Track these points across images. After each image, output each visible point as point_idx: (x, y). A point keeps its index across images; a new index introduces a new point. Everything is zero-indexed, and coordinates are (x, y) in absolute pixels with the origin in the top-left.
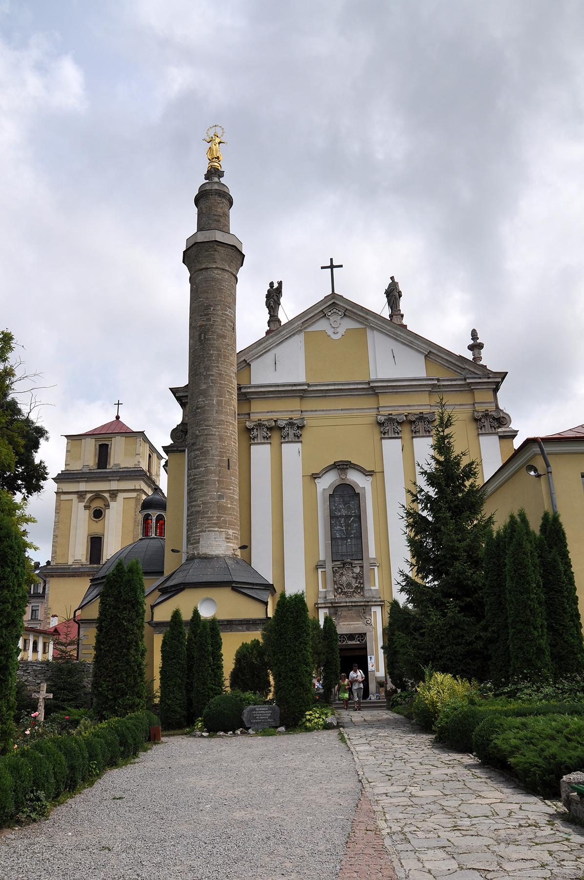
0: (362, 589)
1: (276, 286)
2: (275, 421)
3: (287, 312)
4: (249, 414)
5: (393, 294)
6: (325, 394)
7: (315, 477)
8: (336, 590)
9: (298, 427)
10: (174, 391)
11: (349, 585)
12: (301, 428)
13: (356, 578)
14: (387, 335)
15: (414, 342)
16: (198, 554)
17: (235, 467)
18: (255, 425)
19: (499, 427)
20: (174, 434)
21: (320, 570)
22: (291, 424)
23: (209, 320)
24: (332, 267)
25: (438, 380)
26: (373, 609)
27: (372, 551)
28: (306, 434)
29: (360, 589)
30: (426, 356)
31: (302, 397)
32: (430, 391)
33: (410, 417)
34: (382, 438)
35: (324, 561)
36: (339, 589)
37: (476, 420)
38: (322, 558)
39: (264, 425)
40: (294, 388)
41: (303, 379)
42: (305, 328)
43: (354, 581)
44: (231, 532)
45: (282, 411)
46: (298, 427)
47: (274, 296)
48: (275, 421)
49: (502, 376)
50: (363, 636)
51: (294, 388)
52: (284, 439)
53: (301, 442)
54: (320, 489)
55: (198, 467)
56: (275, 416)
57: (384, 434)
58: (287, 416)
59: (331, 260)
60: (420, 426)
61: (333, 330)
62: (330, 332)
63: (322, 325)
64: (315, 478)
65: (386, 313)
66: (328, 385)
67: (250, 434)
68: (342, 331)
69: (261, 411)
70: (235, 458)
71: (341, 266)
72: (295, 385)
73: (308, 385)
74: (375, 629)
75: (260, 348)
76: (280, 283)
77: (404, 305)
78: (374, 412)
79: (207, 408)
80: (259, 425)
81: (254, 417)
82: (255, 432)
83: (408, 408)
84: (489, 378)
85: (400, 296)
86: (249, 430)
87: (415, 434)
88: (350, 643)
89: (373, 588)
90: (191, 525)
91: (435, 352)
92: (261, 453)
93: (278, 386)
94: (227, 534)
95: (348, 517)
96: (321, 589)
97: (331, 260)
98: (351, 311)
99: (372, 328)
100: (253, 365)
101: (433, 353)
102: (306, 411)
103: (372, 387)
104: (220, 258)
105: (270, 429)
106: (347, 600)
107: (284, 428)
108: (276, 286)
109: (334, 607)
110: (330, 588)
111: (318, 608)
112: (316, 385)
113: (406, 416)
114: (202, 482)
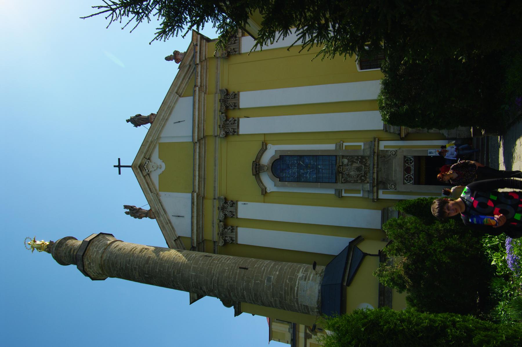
0: (363, 157)
1: (128, 210)
2: (220, 221)
3: (143, 204)
4: (214, 242)
5: (137, 121)
6: (202, 179)
7: (264, 192)
8: (363, 181)
9: (226, 202)
10: (193, 301)
11: (358, 169)
12: (226, 200)
13: (353, 162)
14: (163, 127)
15: (168, 105)
16: (318, 308)
17: (248, 262)
18: (222, 238)
19: (236, 37)
20: (227, 304)
21: (344, 194)
22: (223, 209)
23: (135, 268)
24: (119, 166)
25: (195, 86)
26: (382, 148)
27: (331, 147)
28: (231, 197)
29: (362, 159)
30: (180, 96)
31: (204, 198)
32: (205, 93)
33: (223, 111)
34: (238, 134)
35: (335, 190)
36: (361, 179)
37: (229, 55)
38: (332, 192)
39: (223, 231)
40: (195, 203)
41: (190, 195)
42: (156, 190)
43: (355, 165)
44: (300, 275)
45: (212, 214)
46: (226, 202)
47: (134, 212)
48: (220, 221)
49: (195, 33)
50: (406, 160)
51: (195, 203)
52: (234, 215)
53: (237, 201)
54: (275, 189)
55: (243, 295)
56: (216, 221)
57: (234, 132)
58: (216, 212)
59: (115, 166)
60: (231, 102)
61: (159, 169)
62: (160, 171)
63: (155, 178)
64: (266, 192)
65: (149, 125)
66: (194, 176)
67: (227, 243)
68: (159, 162)
69: (212, 232)
70: (241, 261)
71: (119, 159)
72: (193, 203)
73: (194, 191)
74: (400, 147)
75: (166, 227)
76: (126, 207)
77: (145, 114)
78: (218, 140)
79: (197, 281)
80: (222, 234)
81: (216, 238)
82: (228, 239)
83: (217, 112)
84: (197, 45)
85: (140, 115)
86: (226, 243)
87: (236, 106)
88: (412, 172)
89: (362, 148)
90: (291, 308)
91: (176, 88)
92: (245, 236)
93: (192, 217)
94: (301, 278)
95: (299, 166)
96: (361, 195)
97: (115, 166)
98: (146, 154)
99: (159, 138)
100: (179, 233)
101: (177, 91)
102: (214, 195)
103: (199, 140)
104: (94, 253)
105: (225, 226)
106: (371, 172)
107: (225, 215)
108: (128, 210)
109: (377, 184)
110: (360, 187)
111: (378, 199)
112: (194, 186)
113: (222, 113)
114: (256, 295)
